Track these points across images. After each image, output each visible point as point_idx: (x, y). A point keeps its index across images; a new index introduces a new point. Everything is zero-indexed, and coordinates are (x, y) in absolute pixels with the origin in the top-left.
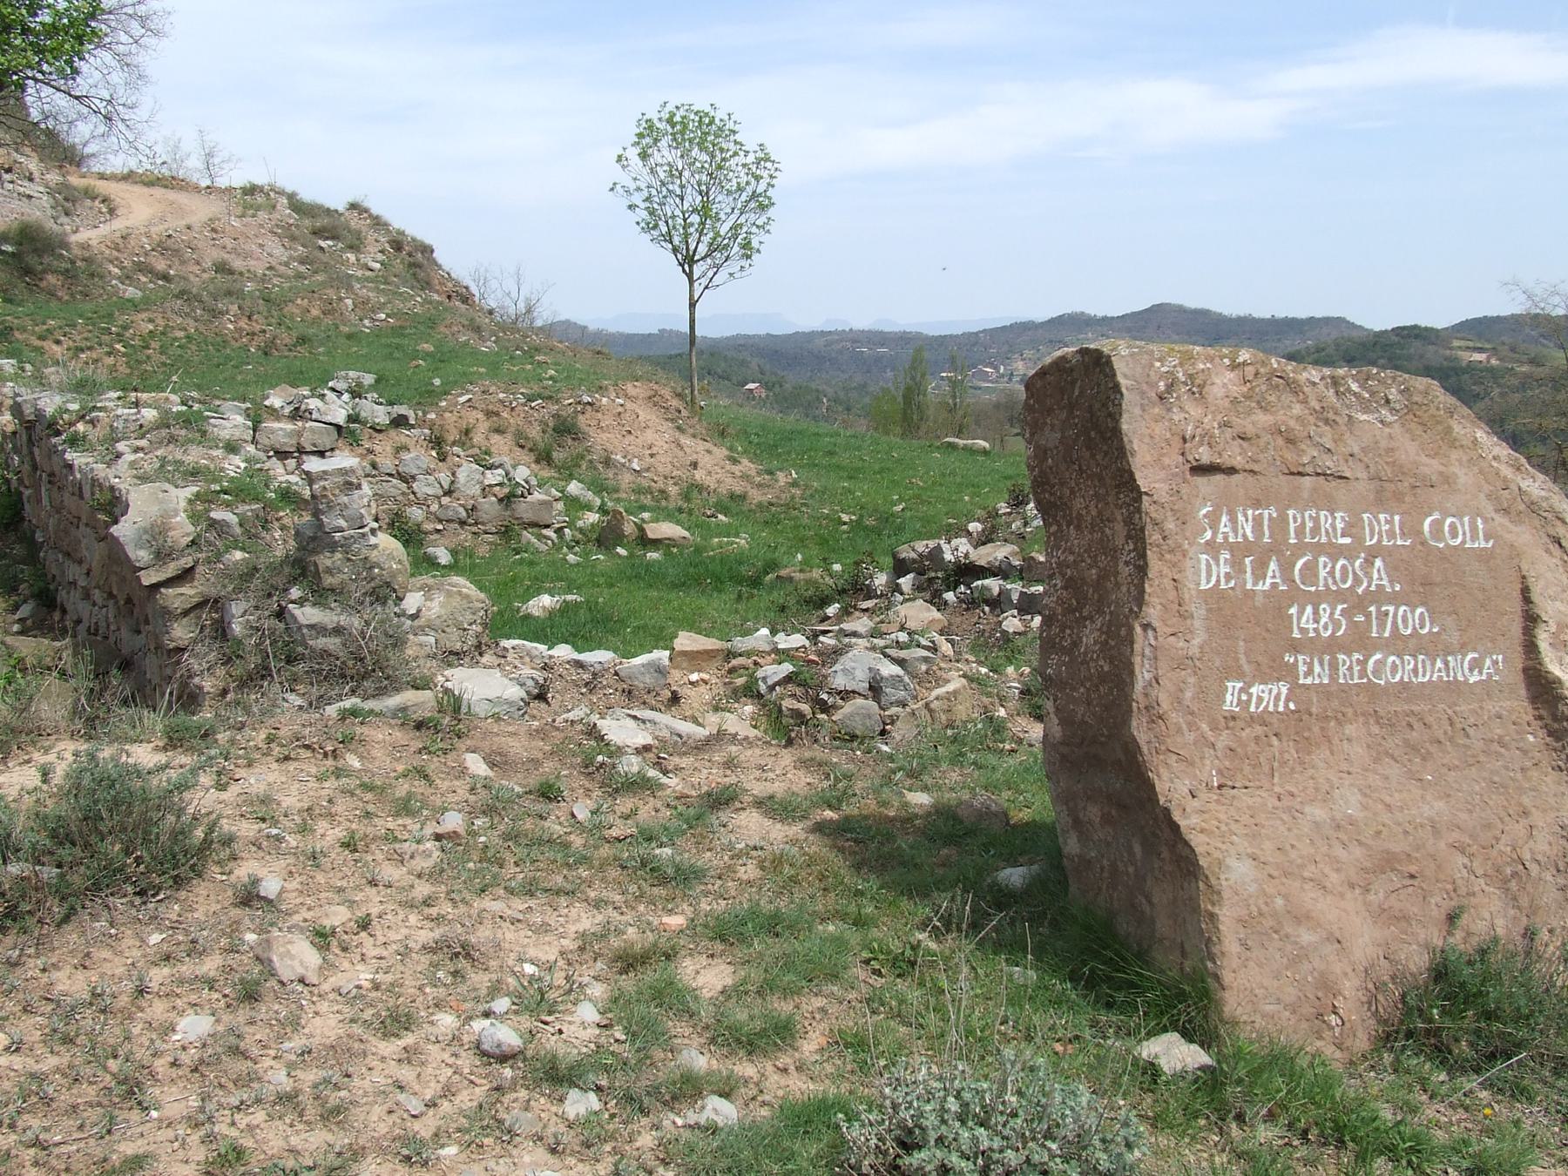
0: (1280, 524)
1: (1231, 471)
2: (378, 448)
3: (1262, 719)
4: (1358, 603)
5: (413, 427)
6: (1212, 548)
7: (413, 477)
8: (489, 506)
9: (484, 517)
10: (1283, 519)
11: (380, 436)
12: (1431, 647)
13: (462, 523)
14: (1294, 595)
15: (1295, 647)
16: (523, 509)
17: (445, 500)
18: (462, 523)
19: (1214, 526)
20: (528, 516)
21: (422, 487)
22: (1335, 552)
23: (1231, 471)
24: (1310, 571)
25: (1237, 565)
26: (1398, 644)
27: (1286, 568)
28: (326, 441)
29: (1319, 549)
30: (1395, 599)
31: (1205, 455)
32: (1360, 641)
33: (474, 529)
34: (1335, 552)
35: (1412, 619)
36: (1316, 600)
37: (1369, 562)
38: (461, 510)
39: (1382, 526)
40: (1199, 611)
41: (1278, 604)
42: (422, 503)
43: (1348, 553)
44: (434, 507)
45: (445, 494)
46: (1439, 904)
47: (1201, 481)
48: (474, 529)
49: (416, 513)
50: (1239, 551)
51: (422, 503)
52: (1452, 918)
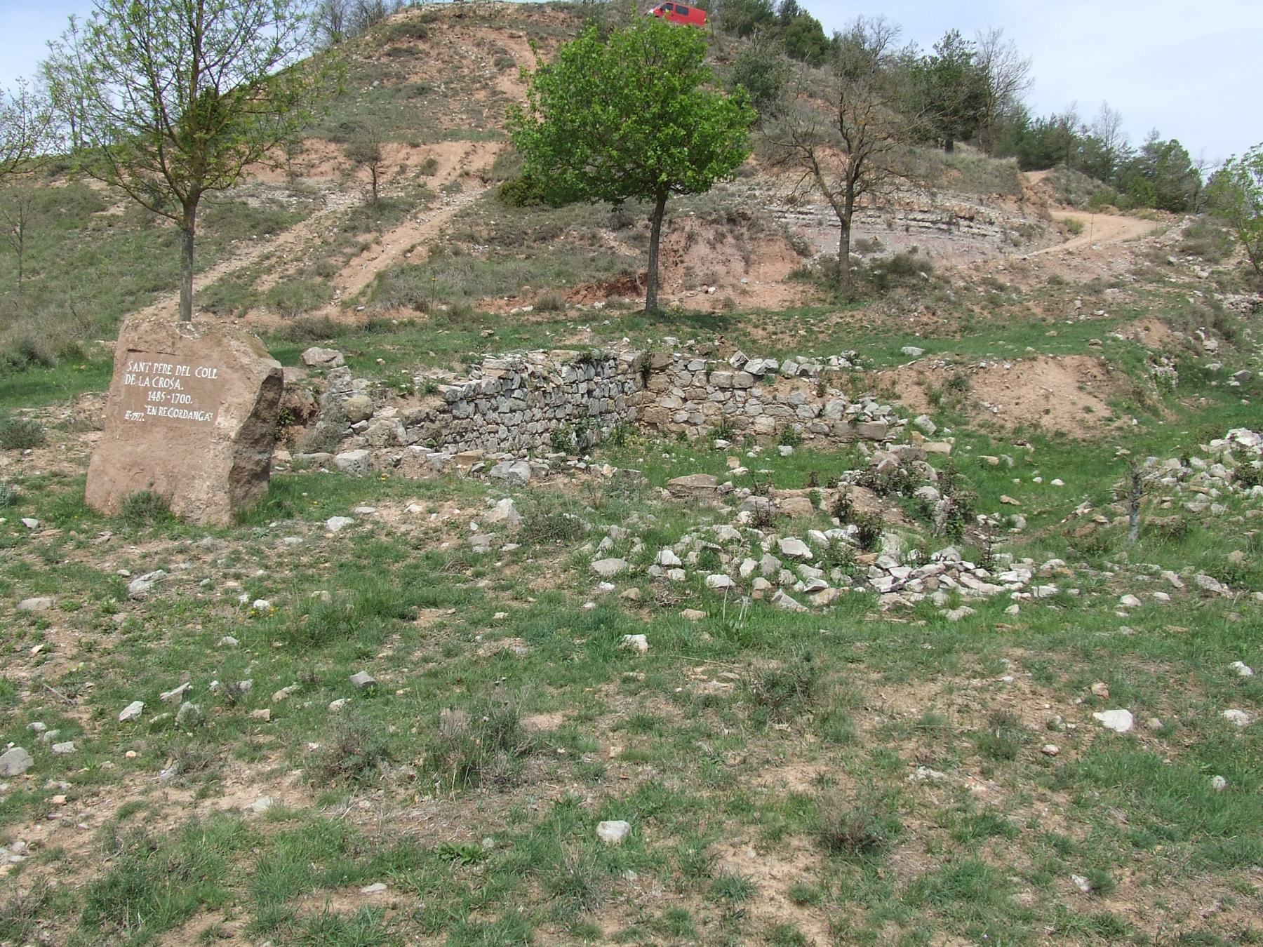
0: (151, 368)
1: (140, 351)
2: (781, 388)
3: (134, 423)
4: (169, 392)
5: (811, 376)
6: (131, 373)
7: (796, 405)
8: (843, 426)
9: (839, 432)
10: (153, 366)
11: (786, 381)
12: (190, 408)
13: (827, 435)
14: (151, 389)
15: (148, 403)
16: (864, 429)
17: (816, 421)
18: (827, 435)
19: (133, 365)
20: (867, 434)
21: (801, 412)
22: (166, 376)
23: (140, 351)
24: (157, 382)
25: (137, 378)
26: (180, 406)
27: (151, 380)
28: (747, 383)
29: (161, 375)
30: (181, 392)
31: (131, 347)
32: (167, 403)
33: (833, 439)
34: (166, 376)
35: (186, 399)
36: (157, 390)
37: (175, 380)
38: (826, 427)
39: (183, 370)
40: (123, 390)
41: (147, 389)
42: (802, 421)
43: (170, 377)
44: (809, 424)
45: (816, 417)
46: (147, 480)
47: (132, 354)
48: (833, 439)
49: (798, 427)
50: (138, 374)
51: (802, 421)
52: (152, 485)
